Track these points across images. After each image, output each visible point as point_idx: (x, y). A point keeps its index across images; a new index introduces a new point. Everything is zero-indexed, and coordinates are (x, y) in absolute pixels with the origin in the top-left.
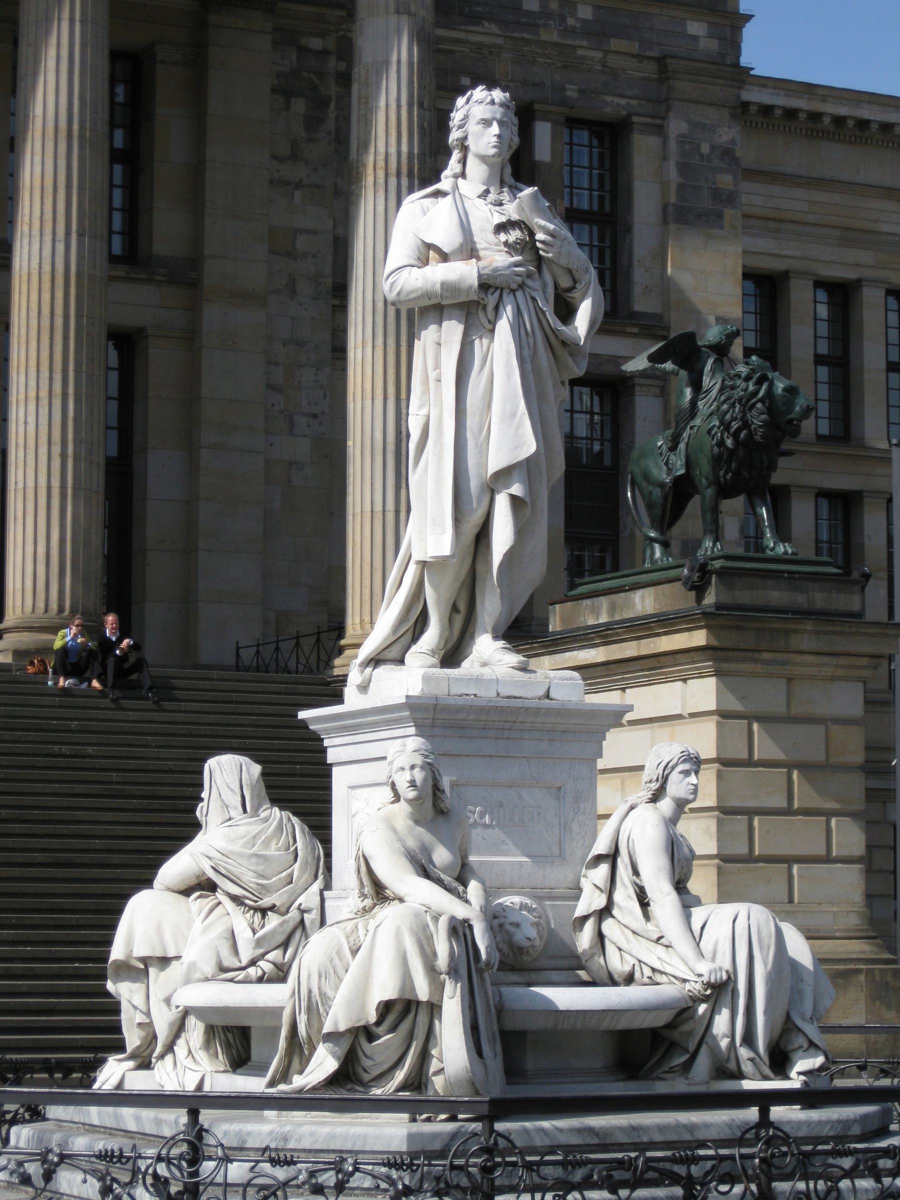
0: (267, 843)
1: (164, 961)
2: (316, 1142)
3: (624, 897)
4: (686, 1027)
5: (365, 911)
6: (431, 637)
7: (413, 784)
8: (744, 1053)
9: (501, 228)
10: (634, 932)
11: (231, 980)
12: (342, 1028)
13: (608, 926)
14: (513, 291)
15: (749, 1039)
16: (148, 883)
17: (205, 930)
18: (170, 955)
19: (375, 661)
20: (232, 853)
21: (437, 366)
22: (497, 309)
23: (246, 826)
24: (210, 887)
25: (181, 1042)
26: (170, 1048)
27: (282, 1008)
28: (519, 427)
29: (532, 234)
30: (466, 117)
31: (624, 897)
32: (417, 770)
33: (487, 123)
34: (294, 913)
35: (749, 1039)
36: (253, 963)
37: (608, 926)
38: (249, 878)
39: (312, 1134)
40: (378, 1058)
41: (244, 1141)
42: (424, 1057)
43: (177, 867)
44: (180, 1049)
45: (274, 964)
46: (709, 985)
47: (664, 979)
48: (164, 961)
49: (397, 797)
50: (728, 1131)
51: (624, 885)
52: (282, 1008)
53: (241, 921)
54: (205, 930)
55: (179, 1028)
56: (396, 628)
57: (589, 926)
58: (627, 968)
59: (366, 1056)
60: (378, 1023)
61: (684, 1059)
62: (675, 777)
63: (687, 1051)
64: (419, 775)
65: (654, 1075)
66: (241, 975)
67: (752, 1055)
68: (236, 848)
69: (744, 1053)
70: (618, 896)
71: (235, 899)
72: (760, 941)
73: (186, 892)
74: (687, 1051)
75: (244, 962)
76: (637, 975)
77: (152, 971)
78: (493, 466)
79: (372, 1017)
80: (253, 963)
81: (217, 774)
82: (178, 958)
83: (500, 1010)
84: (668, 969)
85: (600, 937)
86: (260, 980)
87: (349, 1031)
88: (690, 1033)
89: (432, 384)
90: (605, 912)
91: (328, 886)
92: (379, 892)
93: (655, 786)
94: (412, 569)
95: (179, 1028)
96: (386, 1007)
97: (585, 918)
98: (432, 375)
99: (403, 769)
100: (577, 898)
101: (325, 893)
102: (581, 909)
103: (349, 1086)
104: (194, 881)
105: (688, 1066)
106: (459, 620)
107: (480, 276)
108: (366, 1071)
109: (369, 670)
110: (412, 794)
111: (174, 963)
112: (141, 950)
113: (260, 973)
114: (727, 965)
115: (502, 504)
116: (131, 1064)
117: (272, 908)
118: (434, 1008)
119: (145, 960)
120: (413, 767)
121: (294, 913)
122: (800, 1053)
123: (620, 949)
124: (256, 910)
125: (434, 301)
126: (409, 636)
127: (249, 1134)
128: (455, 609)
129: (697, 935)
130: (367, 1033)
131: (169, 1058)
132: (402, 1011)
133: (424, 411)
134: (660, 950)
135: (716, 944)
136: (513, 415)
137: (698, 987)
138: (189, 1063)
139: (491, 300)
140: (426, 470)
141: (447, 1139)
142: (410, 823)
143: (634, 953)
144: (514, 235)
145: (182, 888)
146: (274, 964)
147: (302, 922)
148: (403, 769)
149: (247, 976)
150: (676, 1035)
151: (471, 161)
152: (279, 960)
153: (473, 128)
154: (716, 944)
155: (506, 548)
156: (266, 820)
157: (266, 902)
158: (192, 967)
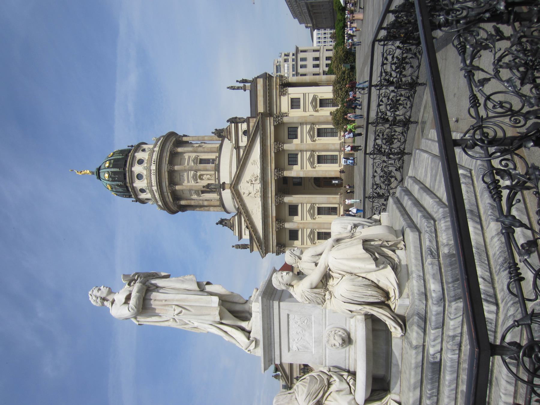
6: (244, 324)
9: (129, 284)
11: (355, 391)
20: (307, 391)
21: (162, 301)
22: (152, 284)
28: (186, 280)
34: (330, 373)
36: (348, 384)
38: (317, 386)
39: (416, 266)
41: (422, 293)
62: (294, 252)
66: (352, 387)
68: (305, 390)
75: (348, 386)
80: (348, 384)
86: (355, 380)
93: (297, 258)
98: (164, 303)
99: (282, 276)
125: (142, 298)
127: (419, 291)
133: (174, 306)
136: (183, 281)
140: (190, 306)
148: (282, 276)
149: (353, 384)
153: (99, 294)
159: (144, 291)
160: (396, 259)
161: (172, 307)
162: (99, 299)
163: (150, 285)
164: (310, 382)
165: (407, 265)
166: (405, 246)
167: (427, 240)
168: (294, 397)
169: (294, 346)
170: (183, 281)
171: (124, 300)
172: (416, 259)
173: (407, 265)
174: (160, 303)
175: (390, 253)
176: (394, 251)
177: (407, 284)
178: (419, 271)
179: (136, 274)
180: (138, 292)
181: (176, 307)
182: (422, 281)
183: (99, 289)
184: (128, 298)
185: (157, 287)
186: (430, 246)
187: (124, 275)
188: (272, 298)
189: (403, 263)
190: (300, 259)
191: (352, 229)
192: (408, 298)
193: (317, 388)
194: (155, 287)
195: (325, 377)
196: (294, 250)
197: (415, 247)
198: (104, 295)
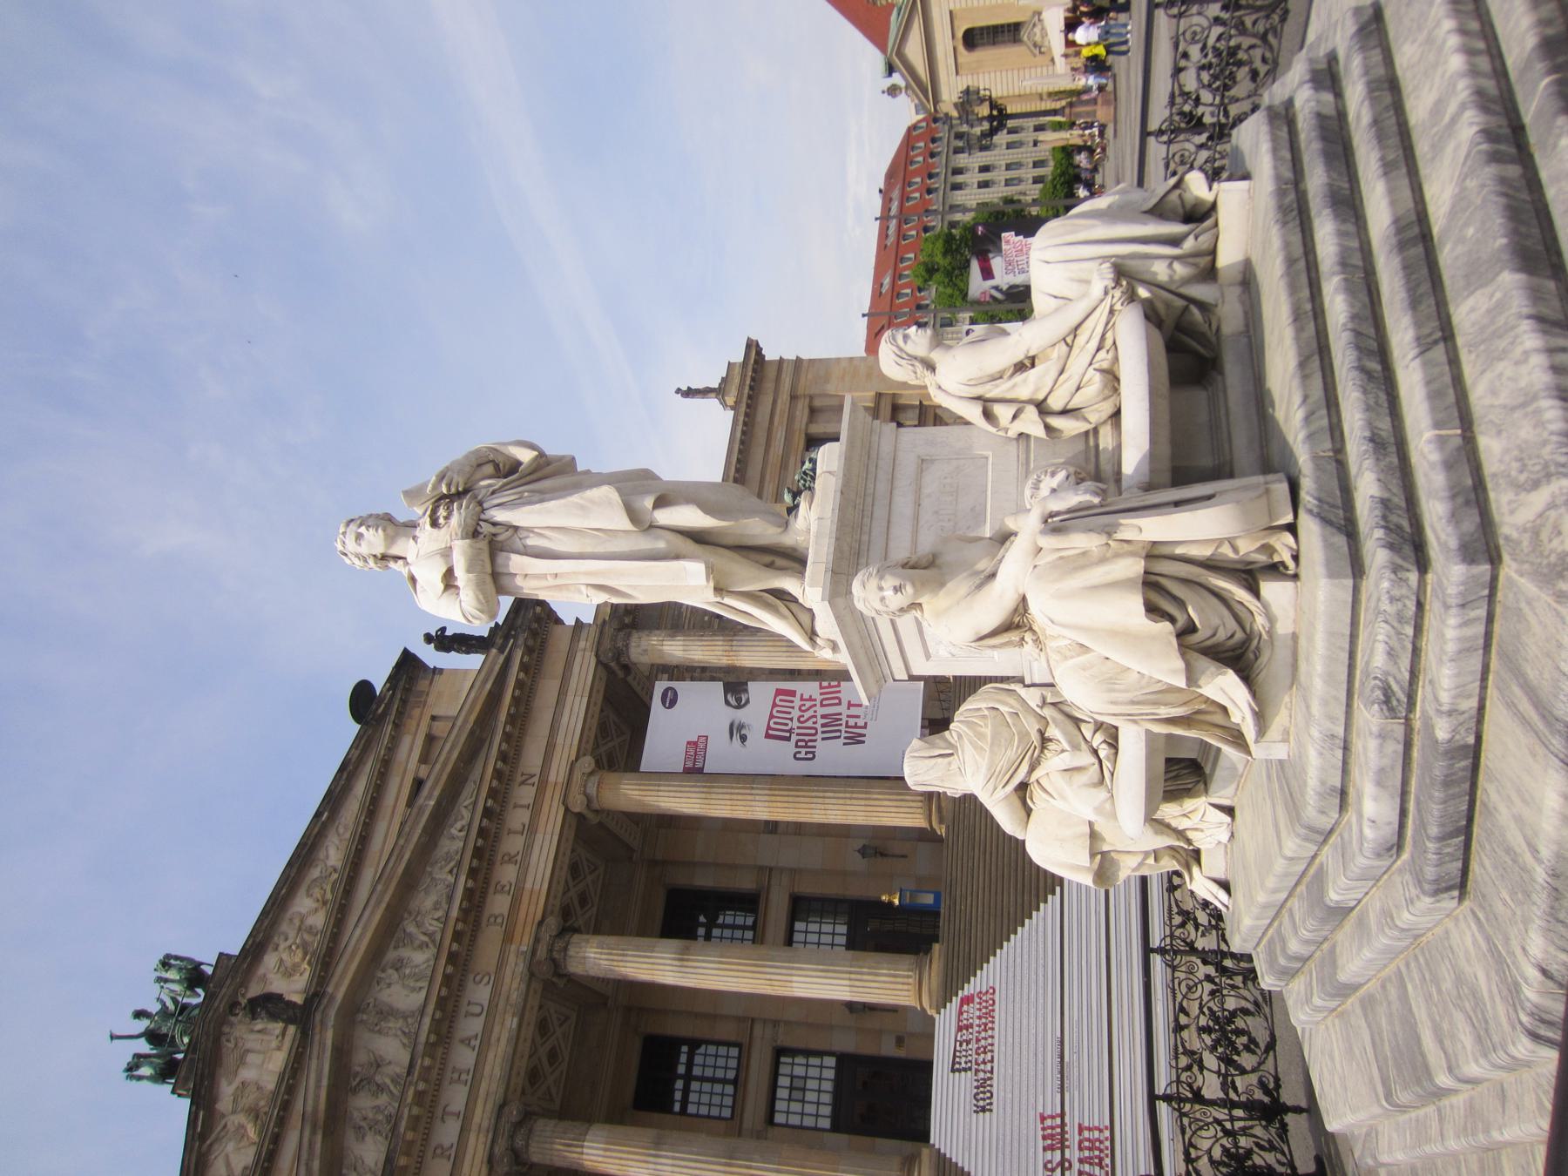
0: (981, 736)
1: (1094, 836)
2: (1336, 699)
3: (1026, 385)
4: (1160, 307)
5: (1037, 641)
6: (789, 584)
7: (897, 589)
8: (1189, 244)
9: (435, 523)
10: (1061, 373)
12: (1180, 664)
13: (1055, 403)
14: (483, 511)
15: (1175, 241)
16: (1021, 844)
17: (1063, 798)
18: (1087, 830)
19: (812, 635)
21: (544, 576)
22: (495, 524)
23: (968, 753)
24: (1023, 787)
25: (1174, 824)
26: (1180, 834)
27: (1148, 732)
28: (592, 502)
29: (443, 497)
30: (357, 556)
31: (1026, 385)
32: (883, 584)
33: (359, 537)
35: (1175, 241)
36: (1095, 752)
37: (1055, 403)
38: (1012, 753)
40: (1216, 621)
41: (1333, 789)
42: (1211, 565)
43: (1006, 818)
44: (1182, 824)
45: (1095, 732)
46: (1117, 283)
47: (1109, 335)
48: (1094, 836)
49: (916, 606)
50: (1291, 225)
51: (1014, 386)
52: (1148, 732)
53: (1054, 763)
54: (1063, 798)
55: (1162, 826)
56: (783, 617)
57: (1055, 422)
58: (1098, 377)
59: (1214, 635)
60: (1172, 620)
61: (1194, 310)
62: (910, 348)
63: (1186, 308)
64: (890, 582)
65: (1214, 339)
66: (1107, 764)
67: (1191, 238)
69: (1189, 244)
70: (1024, 393)
71: (1032, 769)
72: (1072, 232)
73: (1029, 812)
74: (1186, 308)
75: (1094, 760)
76: (1105, 365)
77: (1105, 848)
78: (624, 523)
79: (1166, 626)
80: (1095, 752)
81: (920, 779)
82: (1091, 824)
83: (1149, 487)
84: (1099, 330)
85: (1065, 412)
87: (1183, 655)
88: (1168, 305)
89: (559, 582)
90: (1042, 408)
91: (1021, 680)
92: (1016, 623)
94: (727, 601)
95: (1162, 826)
96: (1152, 610)
97: (1048, 428)
98: (551, 582)
99: (883, 599)
100: (1028, 436)
101: (1028, 682)
102: (1037, 430)
103: (1251, 656)
104: (1017, 803)
105: (1203, 306)
106: (779, 562)
107: (463, 538)
108: (1232, 636)
109: (818, 641)
110: (909, 589)
111: (1097, 828)
112: (1084, 859)
113: (1104, 746)
114: (1093, 265)
115: (665, 517)
116: (1195, 869)
117: (1042, 733)
118: (1153, 552)
119: (1092, 855)
120: (881, 589)
121: (1048, 712)
122: (1187, 196)
123: (1078, 389)
124: (1043, 748)
125: (489, 579)
126: (793, 606)
127: (1323, 783)
128: (770, 566)
129: (1061, 302)
130: (1186, 632)
131: (1190, 834)
132: (1158, 594)
133: (583, 588)
134: (1081, 340)
135: (1073, 280)
136: (582, 507)
137: (1118, 293)
138: (1196, 818)
139: (486, 528)
141: (1329, 528)
142: (942, 593)
143: (1081, 371)
144: (442, 512)
145: (1023, 813)
146: (1095, 732)
147: (1053, 704)
148: (883, 599)
149: (1108, 758)
150: (1169, 323)
151: (395, 551)
152: (1092, 727)
153: (364, 549)
154: (1073, 280)
155: (699, 512)
156: (960, 736)
157: (1035, 737)
158: (1098, 810)
159: (486, 556)
160: (1260, 622)
161: (580, 592)
162: (371, 562)
163: (493, 530)
164: (992, 745)
165: (1295, 637)
166: (1296, 558)
167: (1380, 649)
168: (954, 766)
169: (940, 651)
170: (582, 507)
171: (442, 586)
172: (1329, 678)
173: (1295, 637)
174: (543, 583)
175: (1240, 594)
176: (1255, 592)
177: (1287, 699)
178: (1332, 719)
179: (441, 477)
180: (469, 571)
181: (592, 592)
182: (1339, 754)
183: (359, 537)
184: (449, 578)
185: (516, 528)
186: (1387, 673)
187: (407, 493)
188: (863, 560)
189: (1283, 628)
190: (931, 367)
191: (1106, 293)
192: (1285, 740)
193: (1013, 757)
194: (509, 533)
195: (1033, 728)
196: (906, 337)
197: (1332, 634)
198: (379, 551)
